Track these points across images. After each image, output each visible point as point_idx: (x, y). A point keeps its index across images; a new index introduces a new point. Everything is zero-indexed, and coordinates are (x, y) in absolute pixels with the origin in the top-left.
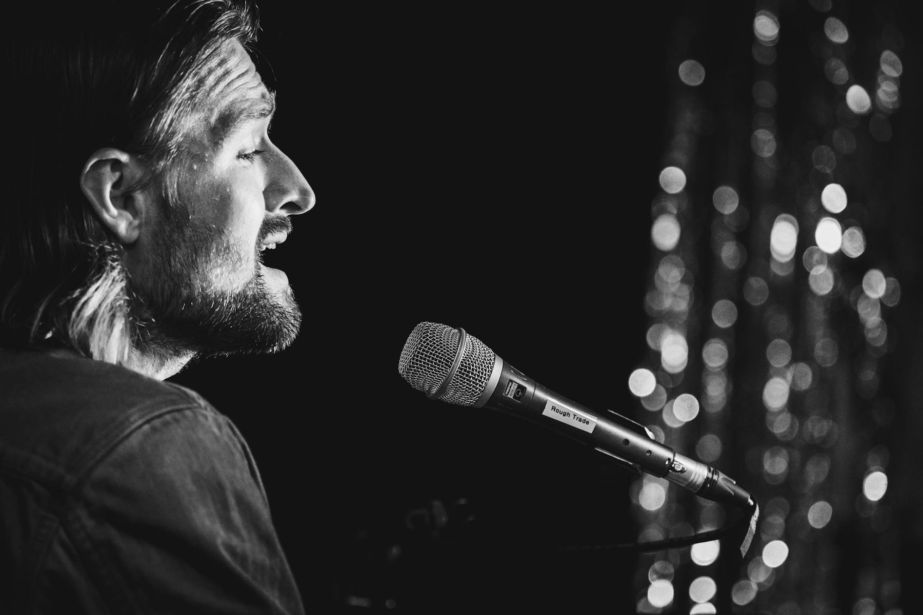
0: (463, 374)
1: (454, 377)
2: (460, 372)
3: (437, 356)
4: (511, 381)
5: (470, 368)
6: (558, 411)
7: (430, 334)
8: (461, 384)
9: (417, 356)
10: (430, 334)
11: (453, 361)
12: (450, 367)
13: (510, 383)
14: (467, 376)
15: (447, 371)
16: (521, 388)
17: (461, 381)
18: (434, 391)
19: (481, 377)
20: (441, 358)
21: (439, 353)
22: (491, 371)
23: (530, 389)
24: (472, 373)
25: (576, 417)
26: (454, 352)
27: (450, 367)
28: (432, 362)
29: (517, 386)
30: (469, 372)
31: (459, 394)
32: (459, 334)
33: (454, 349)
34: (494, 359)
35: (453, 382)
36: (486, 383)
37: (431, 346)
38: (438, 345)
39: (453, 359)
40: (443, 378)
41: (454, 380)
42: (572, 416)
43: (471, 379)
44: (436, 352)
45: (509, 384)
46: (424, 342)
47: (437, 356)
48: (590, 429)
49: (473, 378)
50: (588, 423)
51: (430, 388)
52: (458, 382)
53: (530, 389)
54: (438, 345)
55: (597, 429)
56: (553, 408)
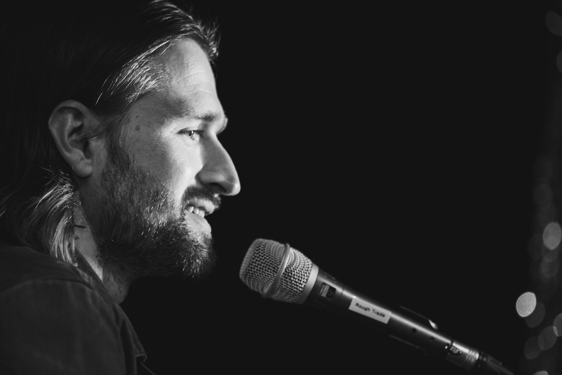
0: (287, 278)
1: (280, 280)
2: (284, 277)
4: (324, 284)
5: (292, 274)
6: (360, 307)
8: (285, 286)
11: (278, 268)
12: (276, 273)
13: (324, 286)
15: (274, 276)
16: (332, 290)
17: (285, 283)
18: (266, 290)
19: (301, 281)
21: (268, 262)
22: (308, 276)
23: (339, 290)
24: (294, 278)
25: (375, 312)
30: (291, 277)
31: (284, 294)
33: (280, 259)
34: (311, 267)
36: (304, 286)
41: (279, 282)
42: (371, 311)
48: (385, 320)
49: (295, 281)
50: (384, 316)
51: (262, 290)
53: (339, 290)
55: (391, 320)
56: (357, 305)
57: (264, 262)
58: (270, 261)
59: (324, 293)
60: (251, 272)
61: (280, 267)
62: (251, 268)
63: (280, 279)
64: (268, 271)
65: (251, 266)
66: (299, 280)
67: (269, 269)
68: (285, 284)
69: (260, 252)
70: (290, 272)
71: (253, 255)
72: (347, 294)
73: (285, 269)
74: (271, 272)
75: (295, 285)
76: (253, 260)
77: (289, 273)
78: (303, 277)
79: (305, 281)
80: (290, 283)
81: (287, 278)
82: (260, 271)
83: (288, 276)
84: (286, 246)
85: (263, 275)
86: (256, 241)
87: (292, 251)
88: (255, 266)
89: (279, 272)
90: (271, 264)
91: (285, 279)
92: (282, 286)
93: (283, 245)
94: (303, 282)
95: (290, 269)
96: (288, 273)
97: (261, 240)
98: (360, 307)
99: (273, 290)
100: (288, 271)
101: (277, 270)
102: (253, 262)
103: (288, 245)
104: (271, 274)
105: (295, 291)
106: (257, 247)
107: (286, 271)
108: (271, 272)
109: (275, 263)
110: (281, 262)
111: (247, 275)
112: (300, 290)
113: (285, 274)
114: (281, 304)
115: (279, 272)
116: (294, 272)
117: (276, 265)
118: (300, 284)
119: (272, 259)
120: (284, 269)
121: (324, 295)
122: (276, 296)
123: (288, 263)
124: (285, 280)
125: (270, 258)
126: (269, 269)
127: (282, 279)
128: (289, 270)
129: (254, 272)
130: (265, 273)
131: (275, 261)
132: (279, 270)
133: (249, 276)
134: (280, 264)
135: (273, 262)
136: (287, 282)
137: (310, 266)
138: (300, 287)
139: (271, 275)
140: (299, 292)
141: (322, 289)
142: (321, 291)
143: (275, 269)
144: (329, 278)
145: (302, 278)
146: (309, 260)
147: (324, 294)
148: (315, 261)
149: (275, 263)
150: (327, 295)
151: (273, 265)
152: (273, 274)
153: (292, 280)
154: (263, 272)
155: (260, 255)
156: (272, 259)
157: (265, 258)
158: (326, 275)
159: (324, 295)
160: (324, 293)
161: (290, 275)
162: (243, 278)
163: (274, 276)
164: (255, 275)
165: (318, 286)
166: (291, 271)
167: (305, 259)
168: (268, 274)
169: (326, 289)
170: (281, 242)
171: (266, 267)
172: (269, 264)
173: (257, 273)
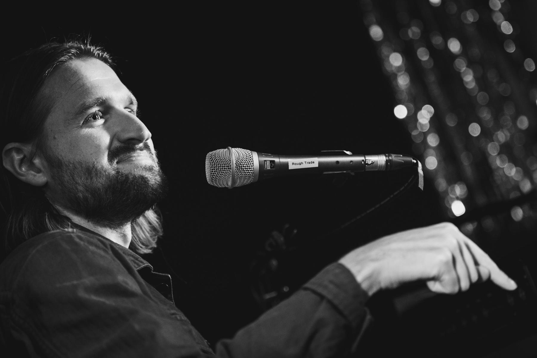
0: (239, 169)
1: (236, 173)
2: (237, 169)
3: (222, 167)
5: (241, 165)
6: (296, 164)
7: (214, 157)
8: (240, 175)
9: (213, 172)
10: (214, 157)
11: (231, 165)
12: (231, 169)
13: (266, 162)
14: (242, 169)
15: (231, 172)
16: (272, 162)
17: (240, 173)
18: (230, 184)
19: (249, 166)
20: (224, 167)
21: (223, 165)
22: (253, 161)
23: (277, 160)
24: (244, 167)
25: (306, 163)
26: (229, 161)
27: (231, 169)
28: (221, 171)
29: (269, 162)
30: (241, 167)
32: (228, 151)
34: (252, 154)
35: (236, 176)
36: (253, 168)
37: (217, 163)
38: (220, 161)
39: (230, 164)
40: (230, 176)
42: (304, 163)
43: (245, 169)
44: (221, 165)
45: (265, 162)
46: (213, 163)
47: (222, 167)
48: (316, 165)
49: (245, 169)
50: (314, 162)
51: (227, 185)
52: (239, 174)
53: (277, 160)
54: (220, 161)
55: (320, 164)
56: (293, 164)
57: (219, 166)
58: (223, 163)
59: (268, 167)
60: (214, 176)
61: (231, 164)
62: (213, 174)
63: (235, 172)
64: (225, 171)
65: (212, 173)
66: (247, 166)
67: (225, 169)
68: (240, 174)
69: (214, 161)
70: (239, 164)
71: (211, 165)
72: (283, 160)
73: (235, 164)
74: (227, 170)
75: (247, 171)
76: (211, 168)
77: (239, 165)
78: (250, 163)
79: (252, 165)
80: (243, 171)
81: (239, 169)
82: (220, 173)
83: (239, 167)
84: (228, 149)
85: (223, 174)
86: (208, 155)
87: (234, 150)
88: (215, 171)
89: (233, 167)
90: (224, 165)
91: (238, 170)
92: (238, 175)
93: (227, 149)
94: (251, 166)
95: (239, 162)
96: (239, 166)
97: (210, 153)
98: (296, 164)
99: (234, 182)
100: (238, 164)
101: (231, 167)
102: (212, 169)
103: (230, 148)
104: (228, 171)
105: (249, 175)
106: (211, 159)
107: (237, 165)
108: (227, 170)
109: (227, 163)
110: (230, 161)
111: (213, 179)
112: (252, 173)
113: (237, 167)
114: (244, 188)
115: (233, 167)
116: (242, 163)
117: (228, 164)
118: (249, 168)
119: (224, 161)
120: (235, 164)
121: (269, 168)
122: (238, 184)
123: (235, 159)
124: (239, 171)
125: (222, 161)
126: (225, 169)
127: (237, 171)
128: (238, 163)
129: (216, 175)
130: (224, 173)
131: (226, 162)
132: (232, 166)
133: (214, 180)
134: (231, 162)
135: (225, 163)
136: (241, 171)
137: (250, 154)
138: (251, 171)
139: (228, 172)
140: (252, 174)
141: (266, 165)
142: (266, 166)
143: (229, 167)
144: (267, 156)
145: (249, 164)
146: (248, 151)
147: (269, 168)
148: (252, 149)
149: (227, 163)
150: (271, 167)
151: (226, 165)
152: (229, 170)
153: (244, 169)
154: (222, 173)
155: (215, 163)
156: (224, 161)
157: (219, 163)
158: (264, 155)
159: (269, 168)
160: (268, 167)
161: (241, 166)
162: (211, 183)
163: (231, 172)
164: (218, 177)
165: (262, 165)
166: (240, 163)
167: (245, 151)
168: (226, 172)
169: (268, 163)
170: (224, 148)
171: (222, 169)
172: (223, 165)
173: (219, 175)
